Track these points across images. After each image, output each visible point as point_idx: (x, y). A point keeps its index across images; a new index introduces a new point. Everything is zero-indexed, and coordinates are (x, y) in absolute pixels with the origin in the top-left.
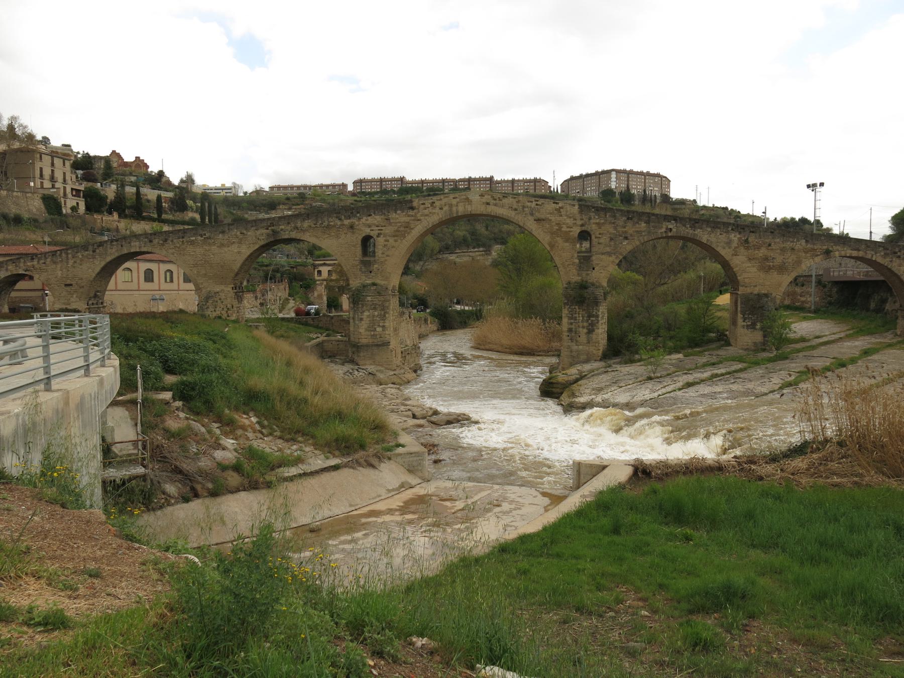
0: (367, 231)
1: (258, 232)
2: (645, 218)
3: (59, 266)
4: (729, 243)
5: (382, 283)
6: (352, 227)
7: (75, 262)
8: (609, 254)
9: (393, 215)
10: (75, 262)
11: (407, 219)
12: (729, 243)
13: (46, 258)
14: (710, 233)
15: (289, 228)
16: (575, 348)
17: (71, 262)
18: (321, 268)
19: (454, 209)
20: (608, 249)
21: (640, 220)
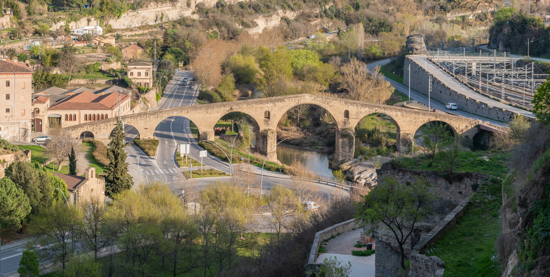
0: (267, 109)
1: (225, 109)
2: (368, 106)
3: (143, 121)
4: (397, 115)
5: (272, 129)
6: (261, 107)
7: (149, 120)
8: (355, 119)
9: (277, 103)
10: (149, 120)
11: (282, 105)
12: (397, 115)
13: (137, 118)
14: (390, 112)
15: (237, 107)
16: (344, 153)
17: (148, 119)
18: (132, 71)
19: (300, 102)
20: (355, 117)
21: (366, 107)
